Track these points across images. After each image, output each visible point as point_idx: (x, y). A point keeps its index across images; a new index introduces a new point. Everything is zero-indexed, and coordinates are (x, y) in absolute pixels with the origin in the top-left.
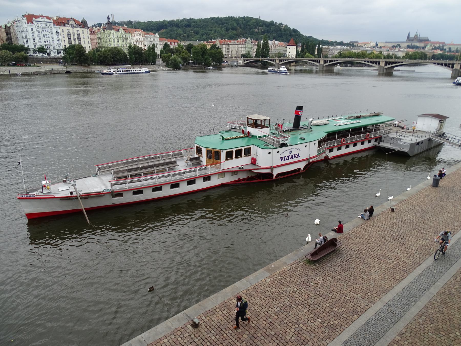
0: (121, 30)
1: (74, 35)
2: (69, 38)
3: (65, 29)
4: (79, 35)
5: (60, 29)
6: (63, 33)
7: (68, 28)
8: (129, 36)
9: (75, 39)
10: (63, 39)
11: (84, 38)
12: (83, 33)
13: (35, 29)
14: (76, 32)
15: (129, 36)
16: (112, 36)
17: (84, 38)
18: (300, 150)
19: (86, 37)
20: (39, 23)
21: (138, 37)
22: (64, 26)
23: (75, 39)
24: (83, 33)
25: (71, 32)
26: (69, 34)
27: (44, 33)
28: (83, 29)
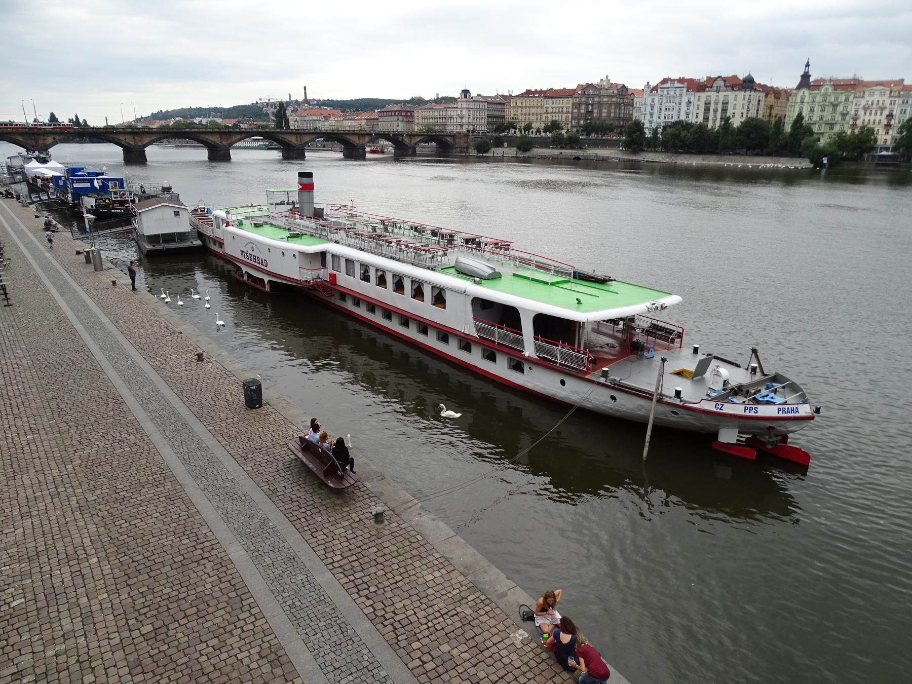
0: (825, 87)
1: (716, 103)
2: (707, 110)
3: (704, 96)
4: (725, 104)
5: (694, 97)
6: (699, 103)
7: (709, 94)
8: (847, 100)
9: (715, 111)
10: (696, 111)
11: (734, 108)
12: (735, 100)
13: (657, 100)
14: (721, 99)
15: (847, 100)
16: (799, 100)
17: (734, 108)
18: (514, 275)
19: (739, 107)
20: (665, 90)
21: (876, 97)
22: (704, 91)
23: (715, 111)
24: (735, 100)
25: (713, 100)
26: (707, 104)
27: (668, 105)
28: (736, 93)
